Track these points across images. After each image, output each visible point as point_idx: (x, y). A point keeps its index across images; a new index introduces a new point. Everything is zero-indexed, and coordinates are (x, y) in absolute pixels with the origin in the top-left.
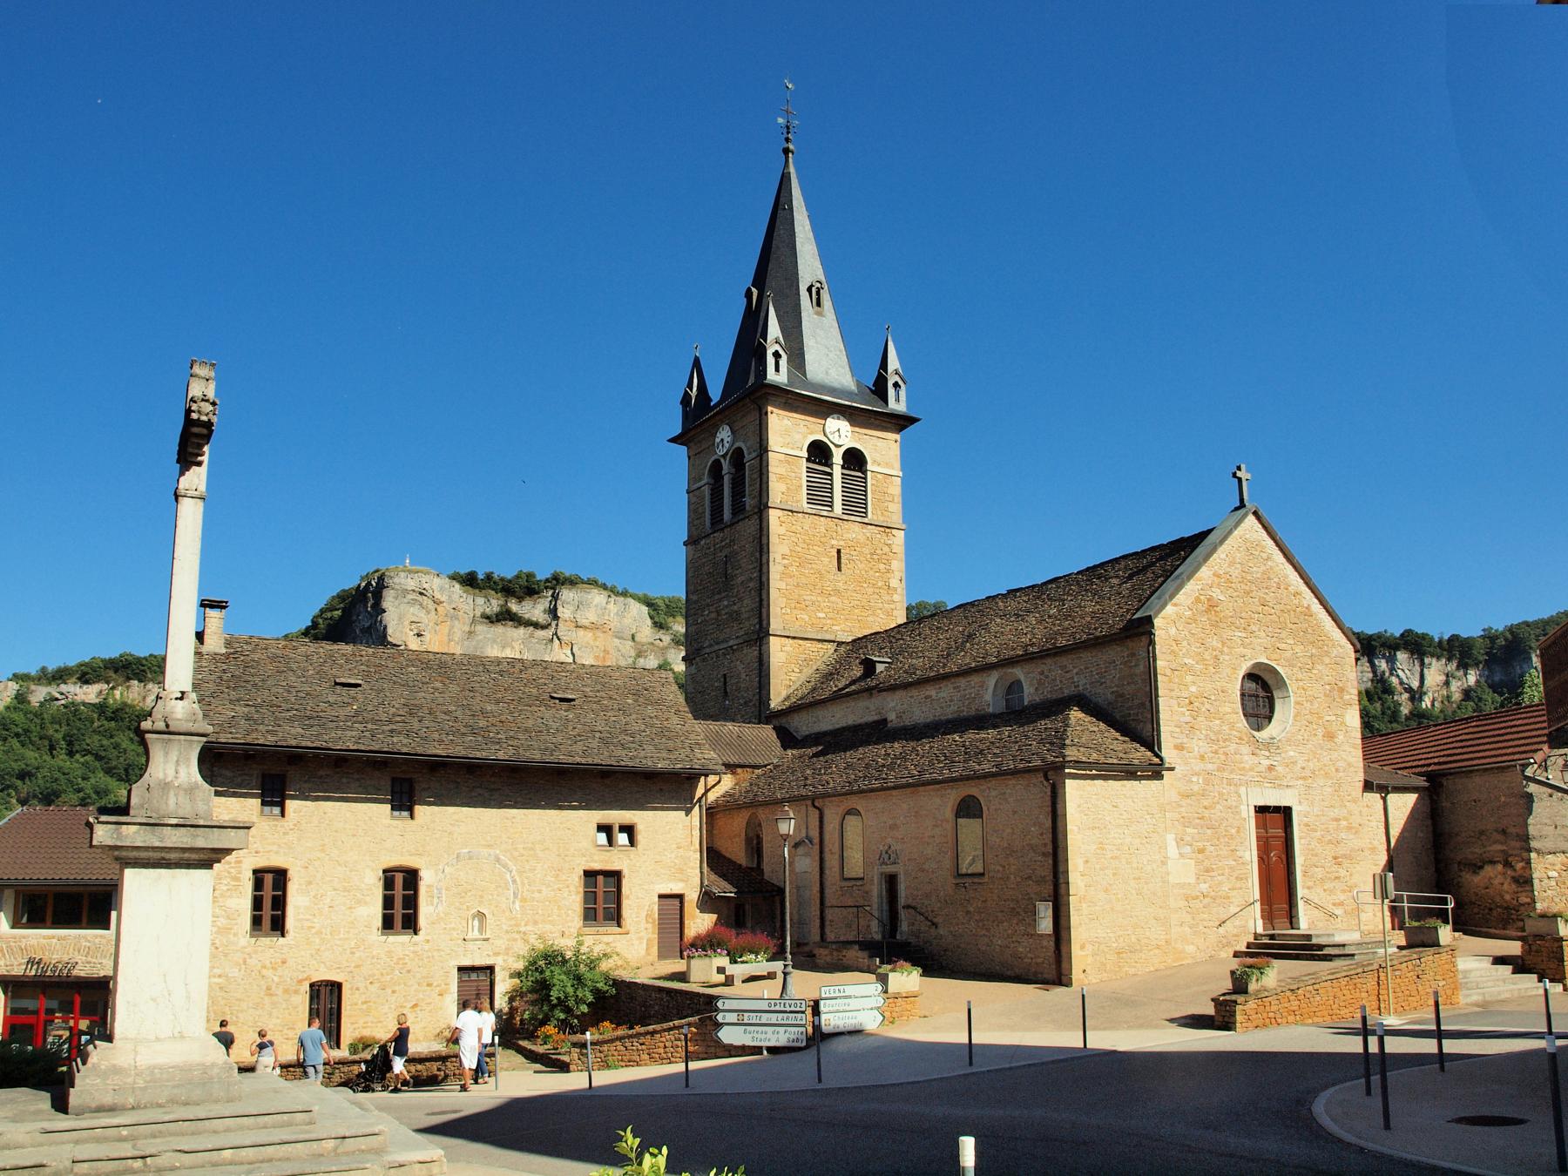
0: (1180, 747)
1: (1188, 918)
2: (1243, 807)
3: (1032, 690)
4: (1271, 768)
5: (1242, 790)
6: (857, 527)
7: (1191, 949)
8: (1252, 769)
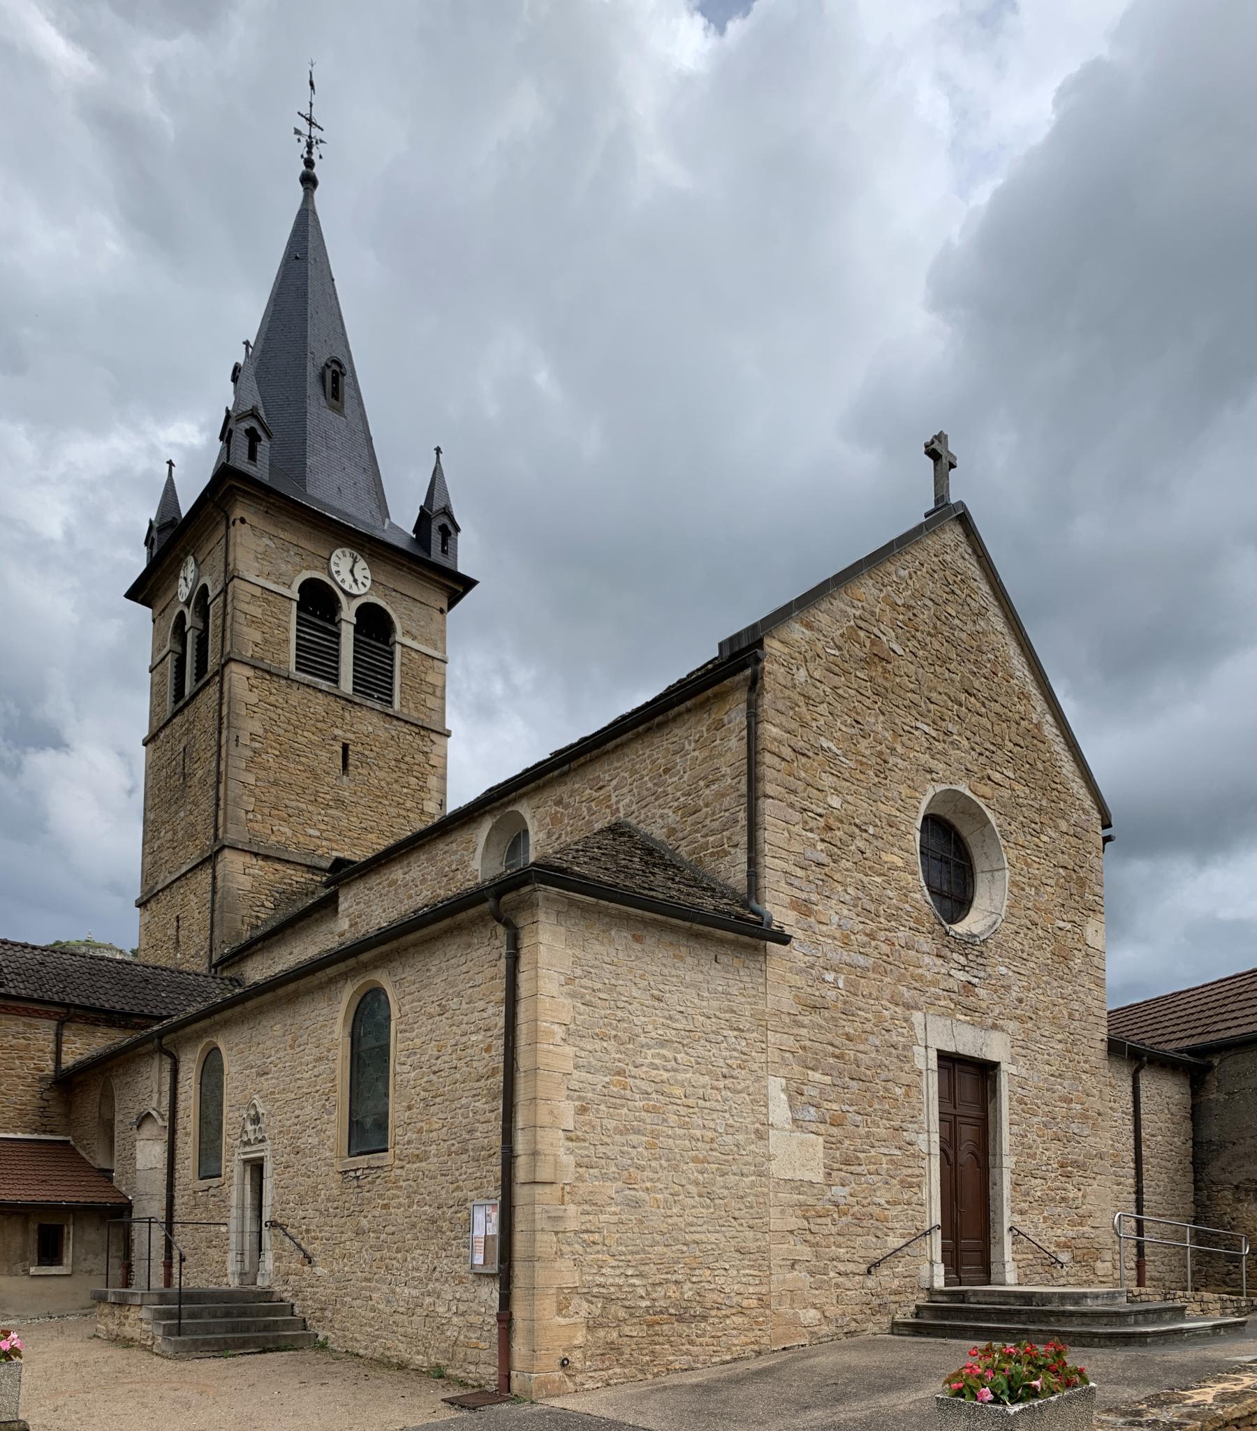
1: (805, 1252)
5: (917, 1017)
7: (811, 1315)
8: (934, 983)
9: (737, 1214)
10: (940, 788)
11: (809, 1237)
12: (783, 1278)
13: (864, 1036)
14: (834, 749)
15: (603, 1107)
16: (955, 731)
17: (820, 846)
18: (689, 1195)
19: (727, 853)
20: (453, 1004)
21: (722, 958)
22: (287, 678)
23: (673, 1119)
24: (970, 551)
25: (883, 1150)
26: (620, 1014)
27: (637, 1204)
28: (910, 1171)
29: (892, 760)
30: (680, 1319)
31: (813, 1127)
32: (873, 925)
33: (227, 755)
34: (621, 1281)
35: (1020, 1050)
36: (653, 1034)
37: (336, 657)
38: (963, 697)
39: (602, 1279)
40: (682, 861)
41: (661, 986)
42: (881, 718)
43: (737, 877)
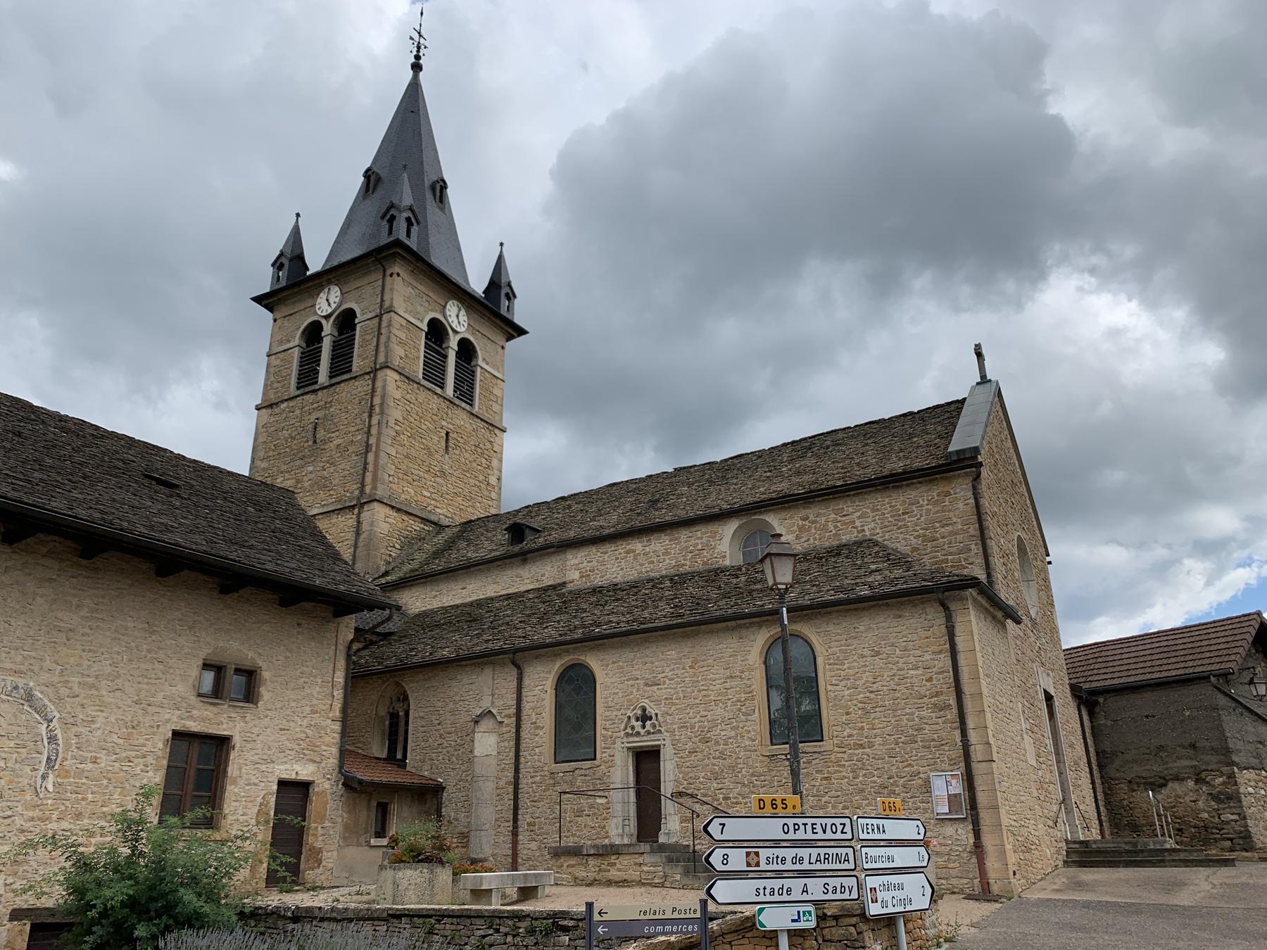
6: (464, 416)
33: (379, 433)
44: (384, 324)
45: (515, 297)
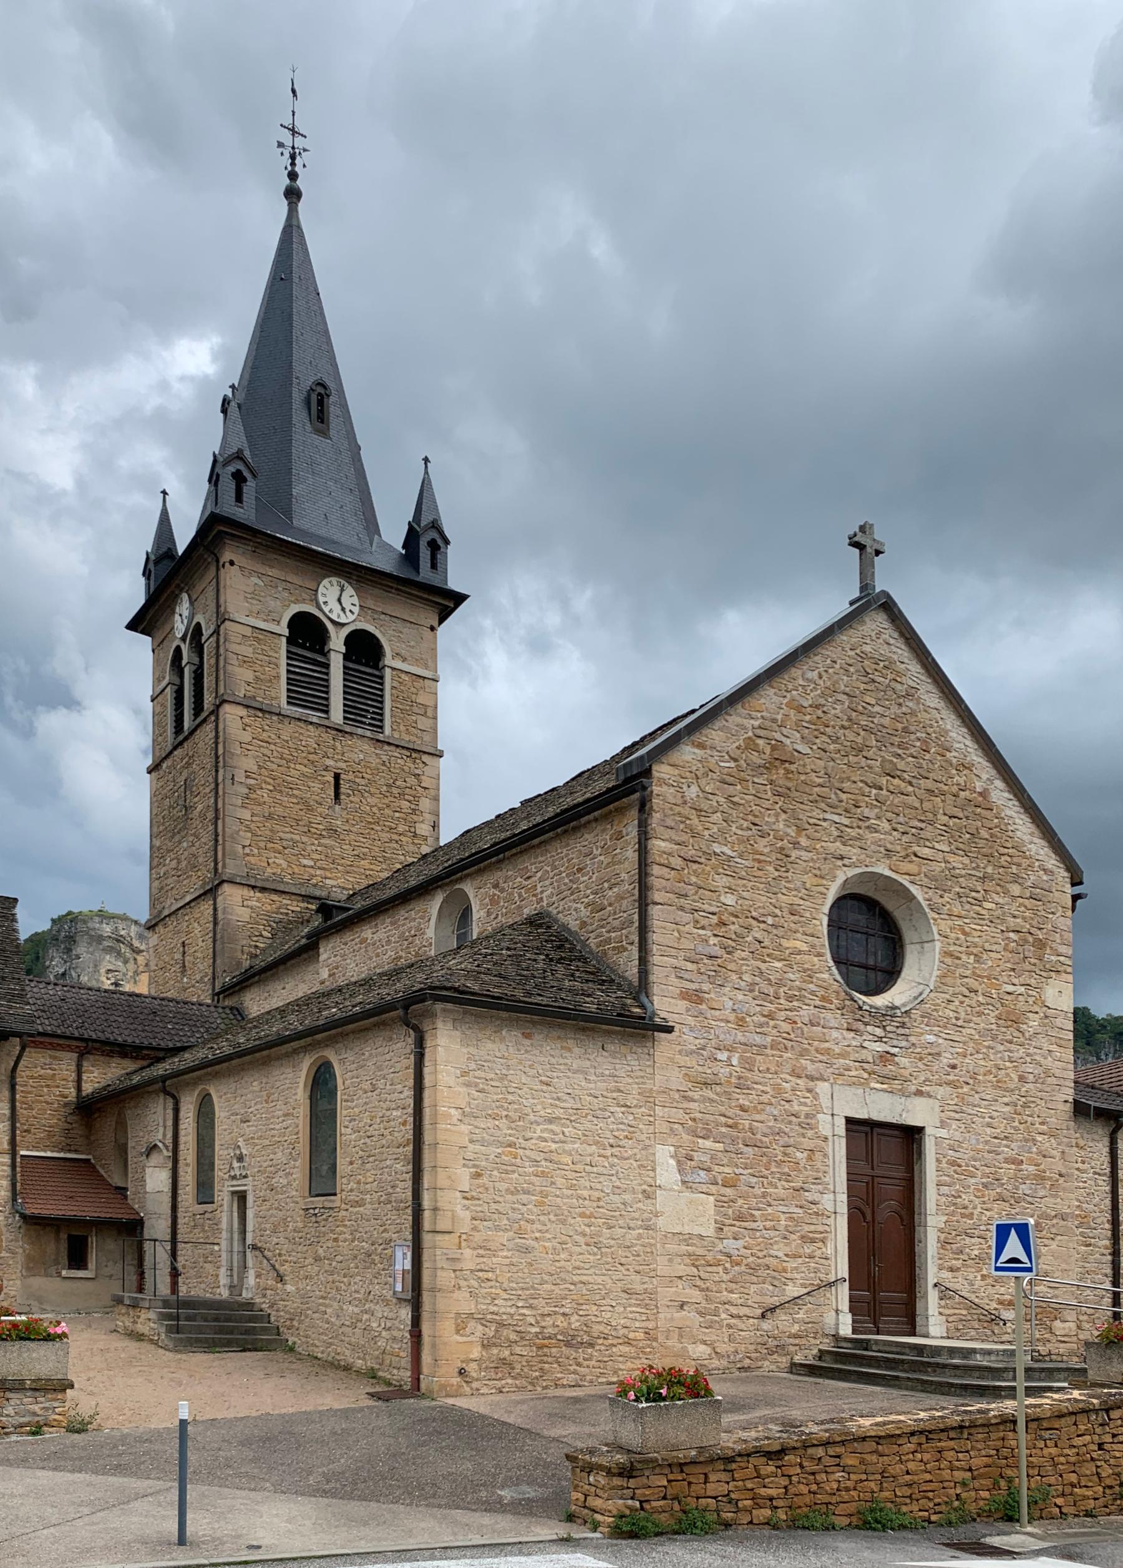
0: (695, 997)
1: (696, 1295)
2: (823, 1120)
3: (483, 913)
4: (886, 1058)
6: (366, 746)
8: (842, 1055)
9: (623, 1260)
10: (851, 872)
11: (699, 1283)
12: (667, 1317)
13: (760, 1107)
14: (729, 853)
15: (495, 1173)
16: (872, 815)
17: (713, 940)
18: (577, 1244)
19: (626, 950)
20: (380, 1084)
21: (608, 1047)
22: (279, 714)
23: (560, 1182)
24: (896, 635)
25: (781, 1208)
26: (510, 1097)
27: (527, 1250)
28: (812, 1228)
29: (794, 854)
30: (568, 1344)
31: (704, 1188)
32: (772, 1007)
34: (513, 1310)
35: (953, 1114)
36: (542, 1113)
37: (326, 688)
38: (884, 781)
39: (495, 1309)
40: (591, 952)
41: (549, 1074)
42: (784, 816)
43: (632, 971)
44: (222, 640)
45: (447, 542)
